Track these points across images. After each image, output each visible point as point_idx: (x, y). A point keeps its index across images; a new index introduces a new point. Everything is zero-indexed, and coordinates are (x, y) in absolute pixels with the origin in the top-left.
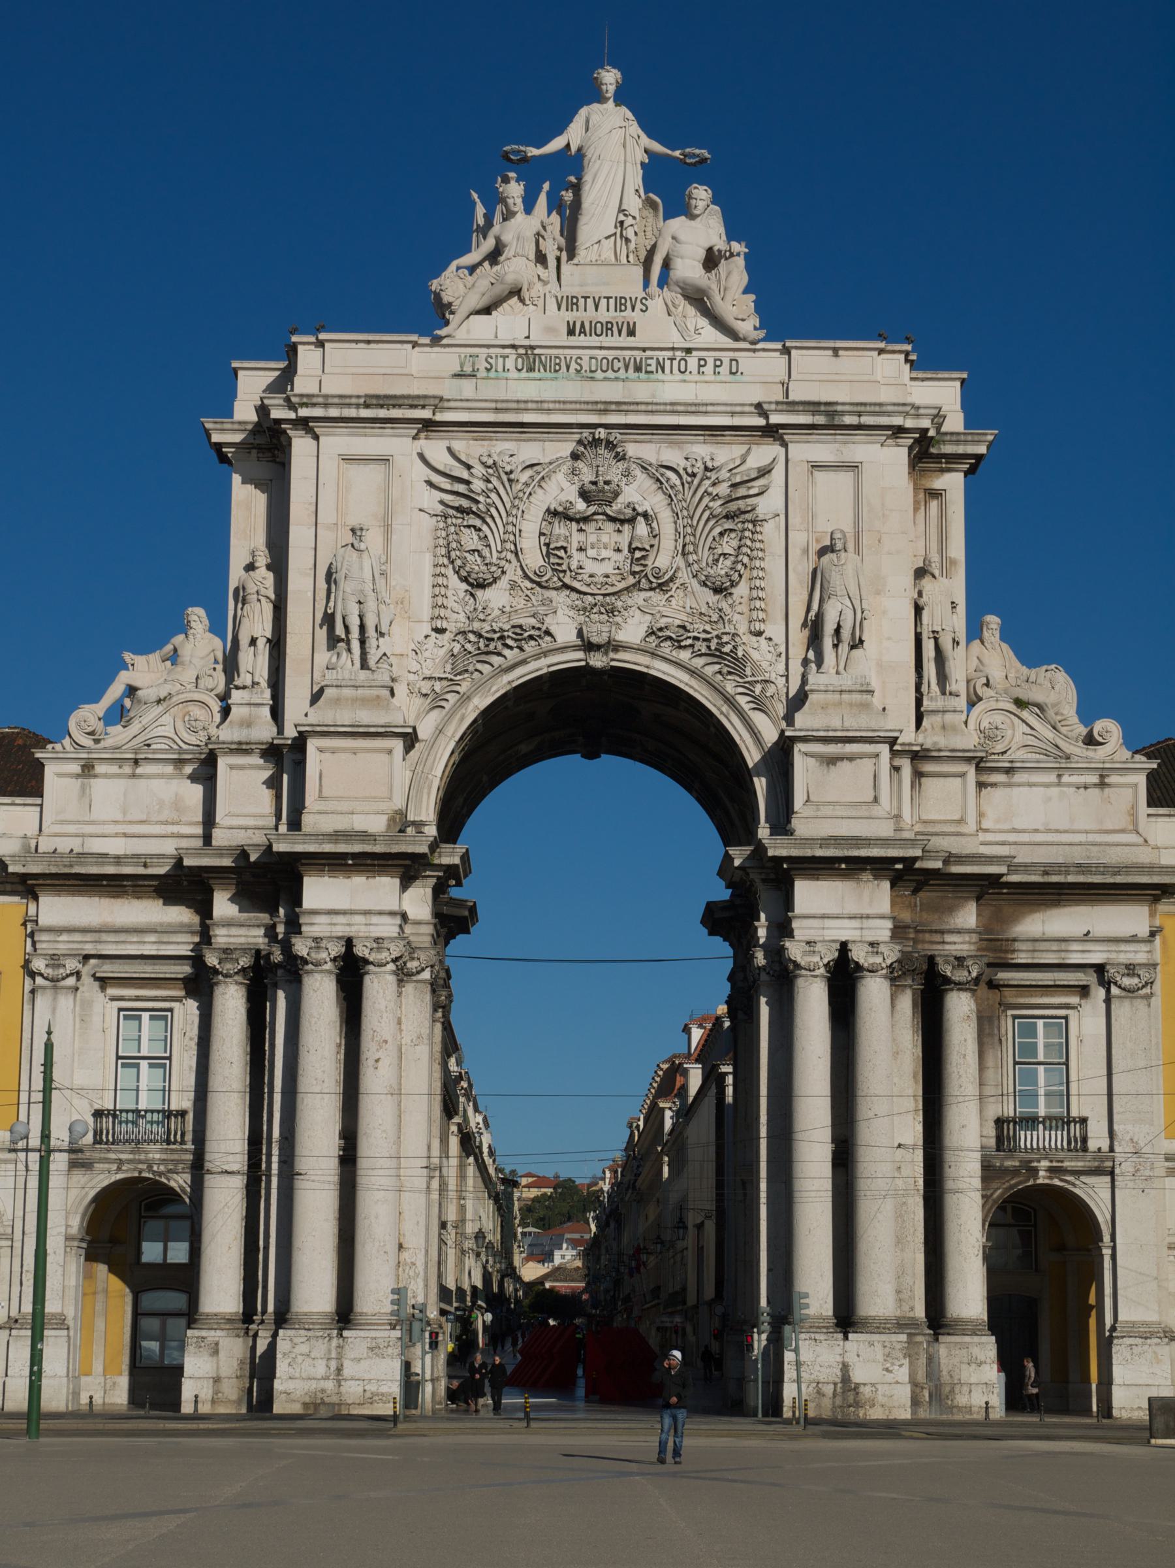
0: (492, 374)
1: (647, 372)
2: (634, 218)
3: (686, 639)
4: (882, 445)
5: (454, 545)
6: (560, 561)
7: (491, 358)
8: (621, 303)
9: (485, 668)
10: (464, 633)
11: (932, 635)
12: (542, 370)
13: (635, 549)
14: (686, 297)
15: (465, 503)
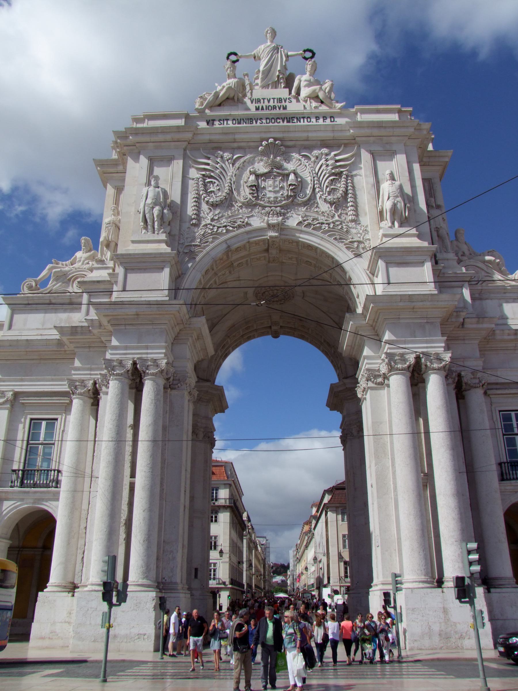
0: (222, 126)
1: (292, 122)
2: (284, 74)
3: (317, 224)
4: (405, 145)
5: (202, 189)
6: (254, 192)
7: (221, 120)
8: (280, 100)
9: (217, 242)
10: (206, 225)
11: (436, 230)
12: (244, 123)
13: (290, 185)
14: (309, 97)
15: (208, 173)
